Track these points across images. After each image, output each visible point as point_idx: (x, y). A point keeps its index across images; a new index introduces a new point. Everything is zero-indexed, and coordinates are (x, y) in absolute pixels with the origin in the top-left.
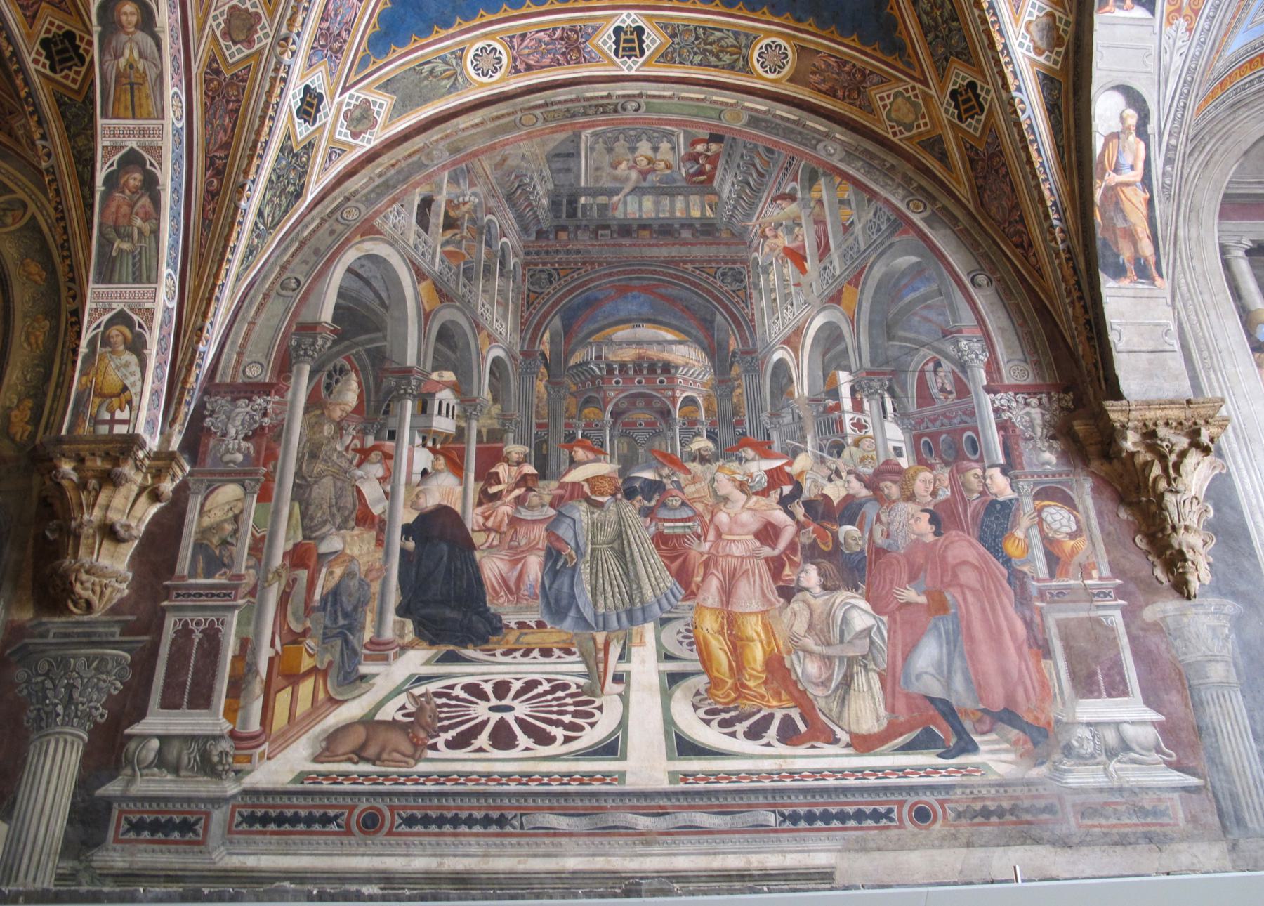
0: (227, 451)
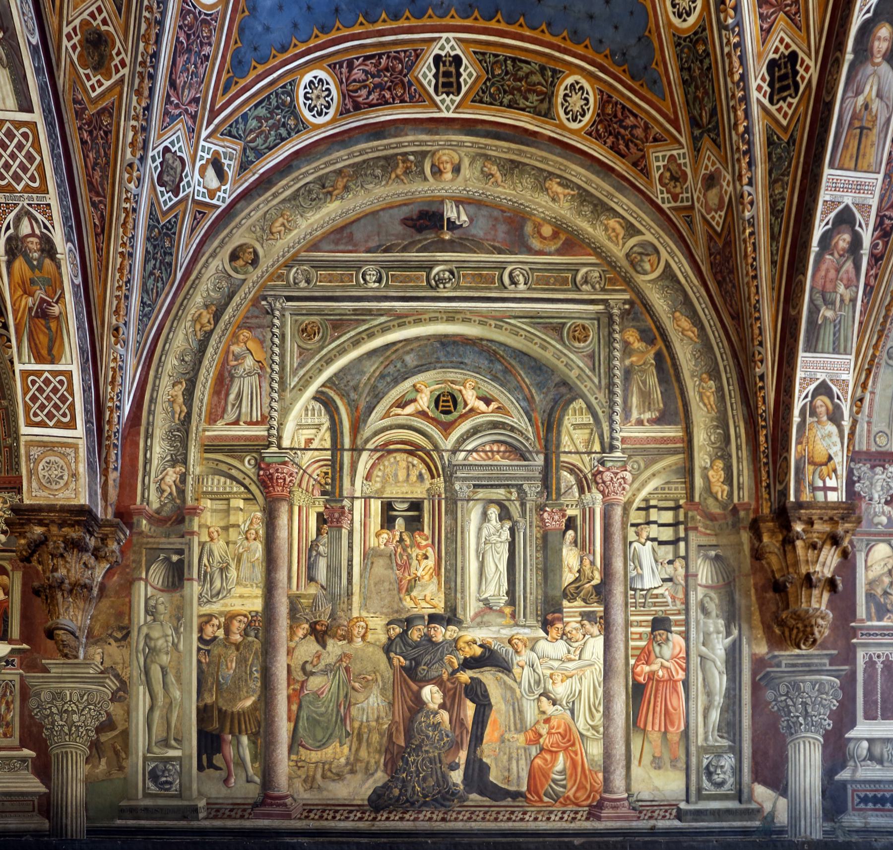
0: (875, 515)
